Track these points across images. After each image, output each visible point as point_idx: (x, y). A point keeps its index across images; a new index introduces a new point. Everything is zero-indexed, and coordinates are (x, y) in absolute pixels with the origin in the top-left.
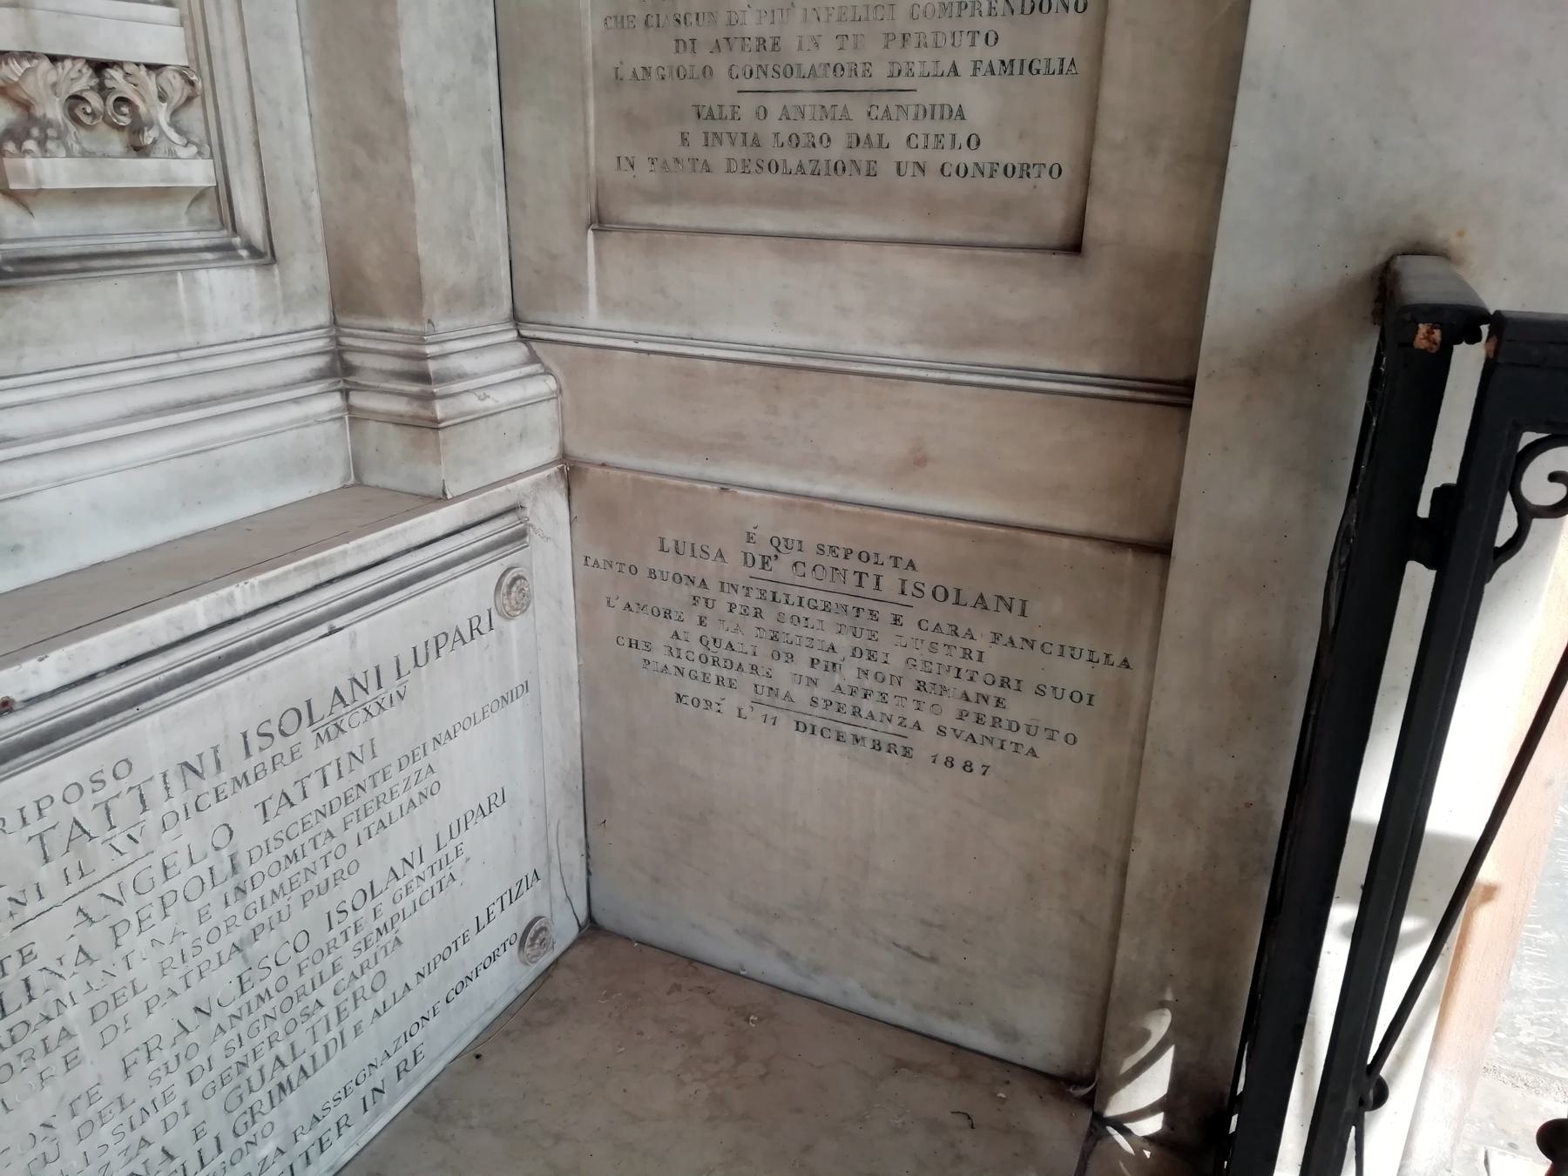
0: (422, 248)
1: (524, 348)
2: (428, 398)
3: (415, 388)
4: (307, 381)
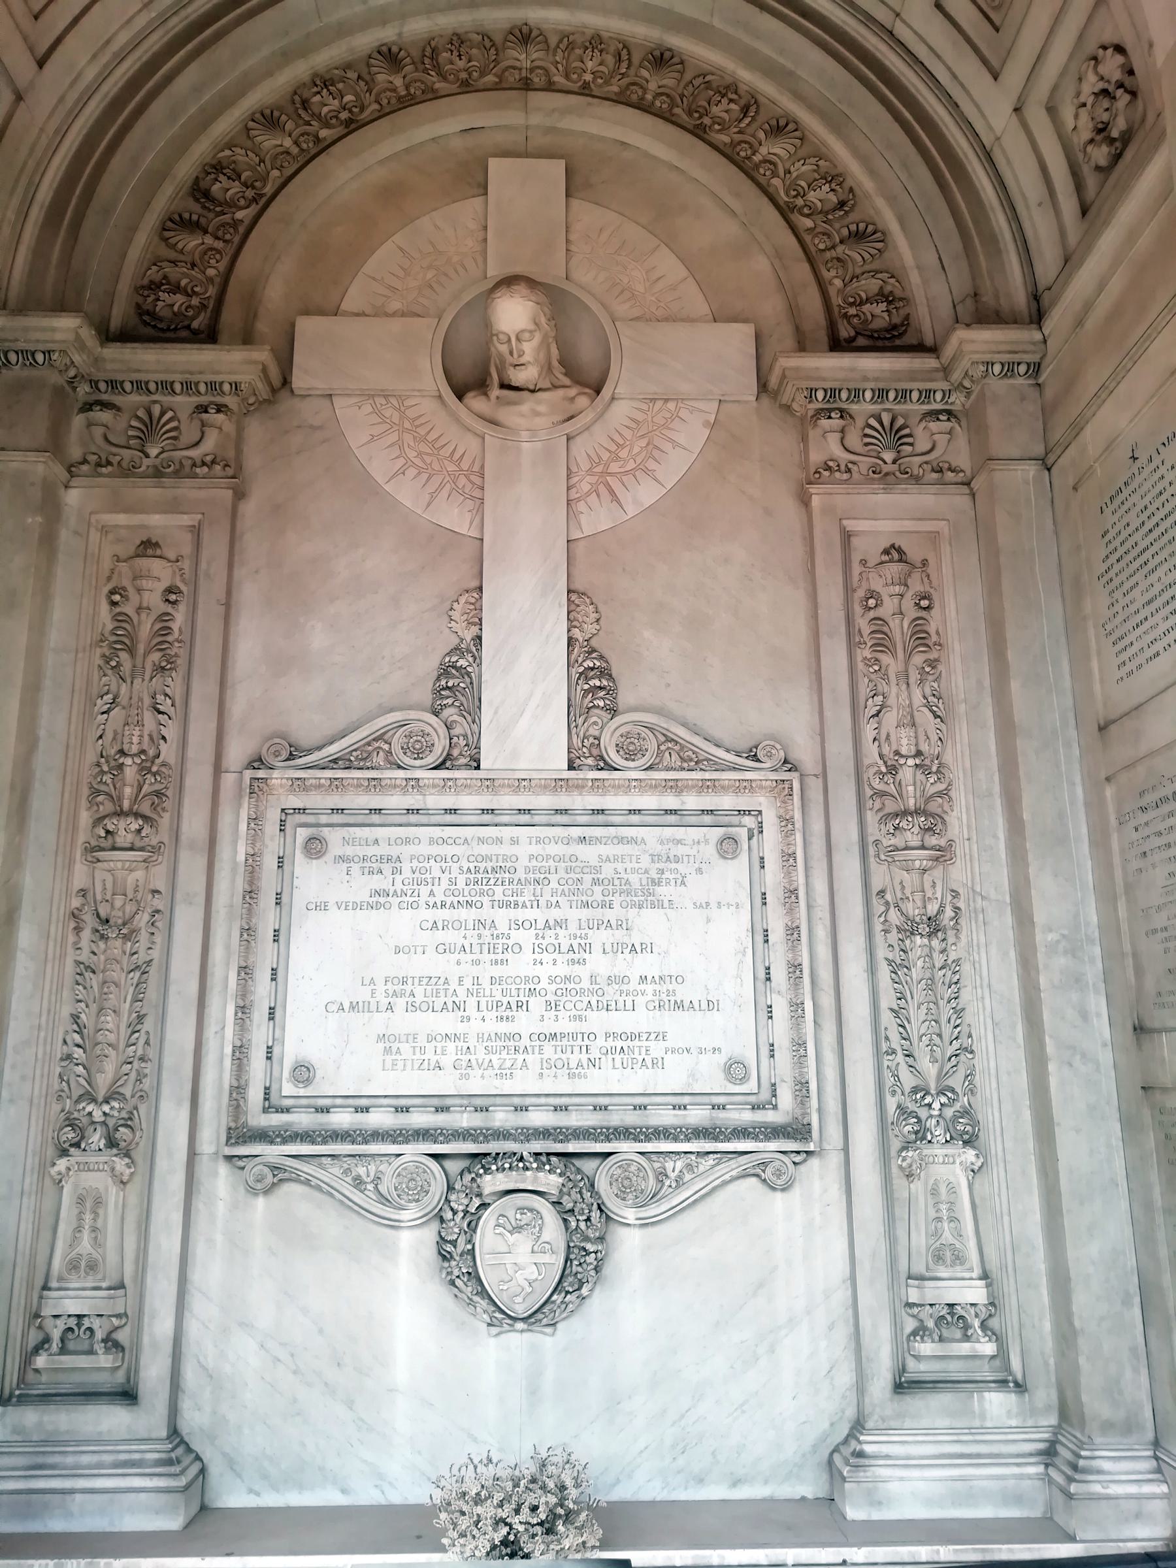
0: (1085, 1398)
1: (1154, 1463)
2: (1070, 1480)
3: (1069, 1472)
4: (1031, 1455)
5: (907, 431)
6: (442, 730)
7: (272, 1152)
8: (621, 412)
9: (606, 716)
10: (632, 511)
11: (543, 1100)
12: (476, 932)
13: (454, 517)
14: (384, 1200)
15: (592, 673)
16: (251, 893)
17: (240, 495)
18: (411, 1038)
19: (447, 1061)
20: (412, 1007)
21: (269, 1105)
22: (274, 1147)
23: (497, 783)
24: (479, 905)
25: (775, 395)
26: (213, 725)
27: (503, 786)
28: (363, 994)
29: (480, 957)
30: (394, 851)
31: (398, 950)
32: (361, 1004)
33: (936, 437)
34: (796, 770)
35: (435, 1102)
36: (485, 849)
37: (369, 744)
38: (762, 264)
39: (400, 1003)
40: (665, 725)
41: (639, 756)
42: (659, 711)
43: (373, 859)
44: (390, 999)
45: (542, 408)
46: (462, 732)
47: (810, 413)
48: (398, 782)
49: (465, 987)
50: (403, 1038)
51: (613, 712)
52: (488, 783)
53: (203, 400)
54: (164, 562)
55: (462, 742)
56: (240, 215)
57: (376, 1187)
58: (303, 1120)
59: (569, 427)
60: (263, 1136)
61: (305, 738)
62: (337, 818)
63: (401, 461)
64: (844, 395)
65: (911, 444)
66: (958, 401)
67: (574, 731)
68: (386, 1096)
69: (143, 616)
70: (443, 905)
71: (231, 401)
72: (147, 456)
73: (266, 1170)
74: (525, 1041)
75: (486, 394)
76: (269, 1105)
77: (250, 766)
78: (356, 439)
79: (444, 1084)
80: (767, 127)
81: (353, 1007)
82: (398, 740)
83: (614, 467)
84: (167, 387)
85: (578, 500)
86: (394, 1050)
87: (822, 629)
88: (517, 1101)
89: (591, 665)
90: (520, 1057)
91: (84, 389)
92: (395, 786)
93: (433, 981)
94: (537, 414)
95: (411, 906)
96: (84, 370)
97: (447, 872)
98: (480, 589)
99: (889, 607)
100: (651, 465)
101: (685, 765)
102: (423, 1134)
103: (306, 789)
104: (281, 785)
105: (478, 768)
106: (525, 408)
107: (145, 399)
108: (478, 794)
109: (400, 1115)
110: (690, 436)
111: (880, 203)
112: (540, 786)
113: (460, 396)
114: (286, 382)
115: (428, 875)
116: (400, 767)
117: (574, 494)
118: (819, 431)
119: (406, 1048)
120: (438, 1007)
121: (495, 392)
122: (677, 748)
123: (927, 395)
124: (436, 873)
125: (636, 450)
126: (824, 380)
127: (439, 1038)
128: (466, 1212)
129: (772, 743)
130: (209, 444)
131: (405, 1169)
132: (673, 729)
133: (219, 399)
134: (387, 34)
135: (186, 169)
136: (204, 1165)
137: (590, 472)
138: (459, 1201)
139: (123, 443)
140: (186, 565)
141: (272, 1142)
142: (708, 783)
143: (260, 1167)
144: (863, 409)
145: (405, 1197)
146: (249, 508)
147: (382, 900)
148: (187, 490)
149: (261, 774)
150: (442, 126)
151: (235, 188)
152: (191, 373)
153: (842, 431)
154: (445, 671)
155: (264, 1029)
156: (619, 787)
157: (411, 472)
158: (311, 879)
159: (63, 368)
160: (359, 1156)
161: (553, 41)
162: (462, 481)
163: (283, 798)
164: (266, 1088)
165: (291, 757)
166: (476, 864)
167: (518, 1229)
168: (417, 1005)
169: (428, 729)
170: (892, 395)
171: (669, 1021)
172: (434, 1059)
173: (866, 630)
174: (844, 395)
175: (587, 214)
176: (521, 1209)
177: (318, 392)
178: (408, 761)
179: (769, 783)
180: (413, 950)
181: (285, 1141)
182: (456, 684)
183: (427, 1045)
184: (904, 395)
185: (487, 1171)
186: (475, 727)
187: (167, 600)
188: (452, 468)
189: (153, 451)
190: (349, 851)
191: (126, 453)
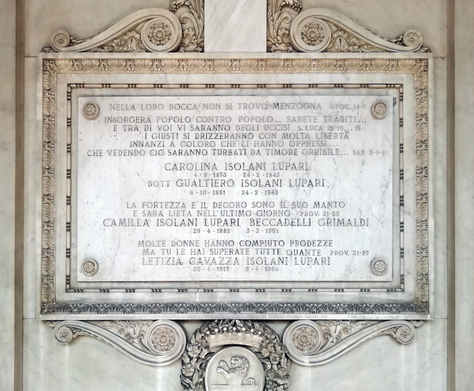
7: (72, 318)
11: (248, 285)
12: (203, 172)
14: (145, 349)
16: (49, 143)
18: (161, 243)
19: (185, 258)
20: (161, 223)
21: (70, 286)
22: (72, 315)
24: (205, 152)
28: (128, 214)
29: (206, 189)
30: (146, 114)
31: (150, 184)
32: (127, 221)
35: (178, 285)
36: (208, 113)
37: (125, 34)
39: (153, 220)
43: (132, 120)
44: (146, 217)
48: (147, 62)
49: (196, 210)
50: (156, 244)
52: (210, 63)
57: (140, 341)
58: (92, 297)
60: (66, 308)
61: (80, 29)
62: (106, 91)
68: (146, 282)
70: (180, 153)
73: (68, 330)
74: (237, 246)
76: (70, 286)
79: (183, 274)
81: (122, 222)
82: (145, 30)
86: (150, 251)
88: (231, 285)
90: (234, 257)
93: (175, 205)
95: (159, 153)
97: (183, 129)
102: (170, 307)
103: (83, 68)
109: (155, 294)
115: (169, 131)
116: (147, 51)
119: (157, 250)
120: (179, 222)
124: (175, 130)
127: (179, 243)
128: (198, 358)
131: (159, 329)
136: (29, 327)
138: (194, 351)
141: (71, 312)
143: (64, 328)
145: (159, 348)
147: (138, 149)
155: (63, 237)
158: (89, 134)
160: (129, 321)
163: (68, 76)
164: (67, 276)
165: (71, 43)
166: (202, 123)
167: (232, 370)
168: (164, 221)
171: (337, 235)
172: (177, 257)
176: (235, 357)
180: (160, 183)
181: (79, 311)
183: (172, 248)
185: (212, 332)
190: (115, 114)
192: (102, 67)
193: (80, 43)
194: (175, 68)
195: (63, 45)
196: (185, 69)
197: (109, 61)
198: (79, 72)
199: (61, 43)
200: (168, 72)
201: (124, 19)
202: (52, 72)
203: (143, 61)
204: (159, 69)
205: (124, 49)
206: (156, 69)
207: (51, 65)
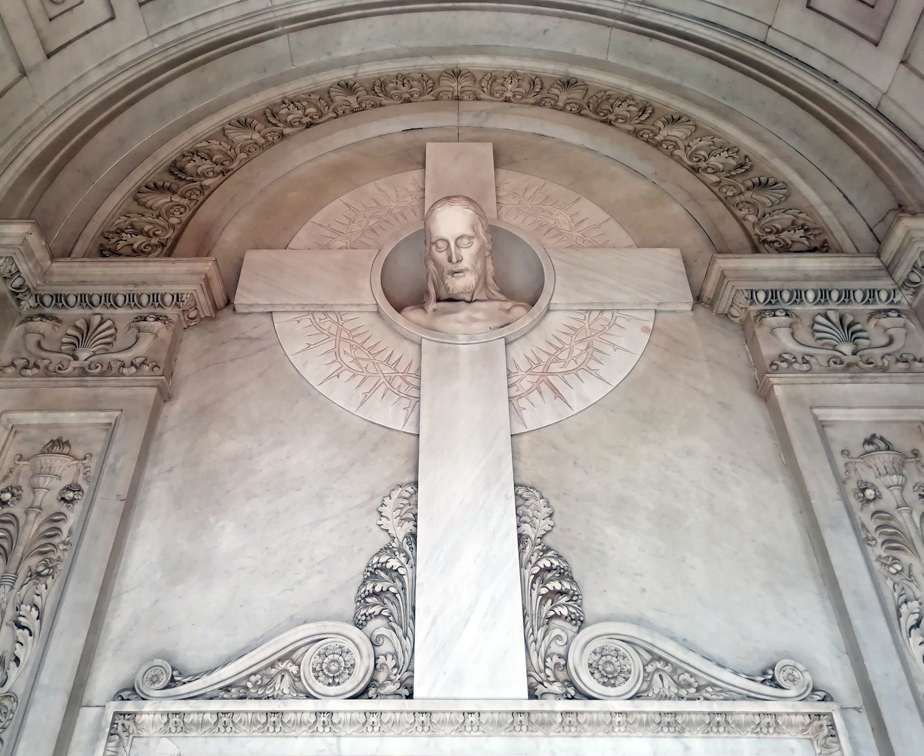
5: (858, 327)
6: (366, 647)
8: (557, 321)
9: (571, 628)
10: (577, 406)
13: (390, 414)
15: (549, 575)
17: (165, 396)
23: (435, 718)
25: (711, 304)
26: (80, 642)
27: (442, 722)
33: (892, 332)
34: (832, 700)
37: (272, 665)
38: (676, 210)
40: (649, 639)
41: (620, 679)
42: (639, 622)
45: (479, 315)
46: (392, 650)
47: (753, 314)
48: (306, 717)
51: (579, 622)
52: (423, 718)
53: (144, 311)
54: (69, 460)
55: (391, 663)
56: (207, 182)
59: (506, 332)
61: (192, 659)
63: (337, 366)
64: (786, 296)
65: (867, 338)
66: (904, 301)
67: (532, 647)
69: (32, 516)
71: (171, 312)
72: (76, 358)
75: (423, 308)
77: (119, 697)
78: (293, 348)
80: (664, 119)
82: (309, 659)
83: (555, 368)
84: (110, 300)
85: (520, 397)
87: (822, 521)
89: (548, 565)
91: (29, 302)
92: (301, 723)
94: (475, 320)
96: (32, 282)
98: (416, 484)
99: (889, 501)
100: (593, 365)
101: (683, 692)
103: (184, 728)
104: (153, 724)
105: (410, 696)
106: (461, 316)
107: (87, 312)
108: (411, 735)
110: (626, 348)
111: (777, 163)
112: (493, 723)
113: (399, 309)
114: (229, 302)
116: (309, 696)
117: (514, 391)
118: (765, 330)
121: (432, 305)
122: (668, 669)
123: (871, 295)
125: (576, 352)
126: (766, 279)
129: (792, 662)
130: (142, 348)
132: (659, 644)
133: (159, 311)
134: (346, 74)
135: (167, 153)
137: (530, 371)
139: (56, 348)
140: (93, 463)
142: (718, 718)
144: (808, 308)
146: (173, 411)
148: (111, 389)
149: (129, 707)
150: (388, 125)
151: (206, 166)
152: (136, 285)
153: (790, 326)
154: (372, 574)
156: (598, 724)
157: (346, 375)
159: (8, 275)
161: (479, 77)
162: (398, 382)
165: (172, 683)
169: (348, 645)
170: (835, 295)
173: (872, 525)
174: (786, 296)
175: (511, 179)
177: (261, 310)
178: (320, 687)
179: (799, 718)
182: (385, 591)
184: (847, 296)
186: (407, 643)
187: (63, 499)
188: (387, 370)
189: (83, 354)
191: (56, 358)
192: (220, 725)
193: (190, 682)
194: (357, 727)
195: (157, 686)
196: (376, 729)
197: (235, 716)
198: (176, 734)
199: (154, 683)
200: (343, 734)
201: (274, 640)
202: (124, 735)
203: (299, 715)
204: (327, 729)
205: (267, 692)
206: (321, 729)
207: (126, 723)
